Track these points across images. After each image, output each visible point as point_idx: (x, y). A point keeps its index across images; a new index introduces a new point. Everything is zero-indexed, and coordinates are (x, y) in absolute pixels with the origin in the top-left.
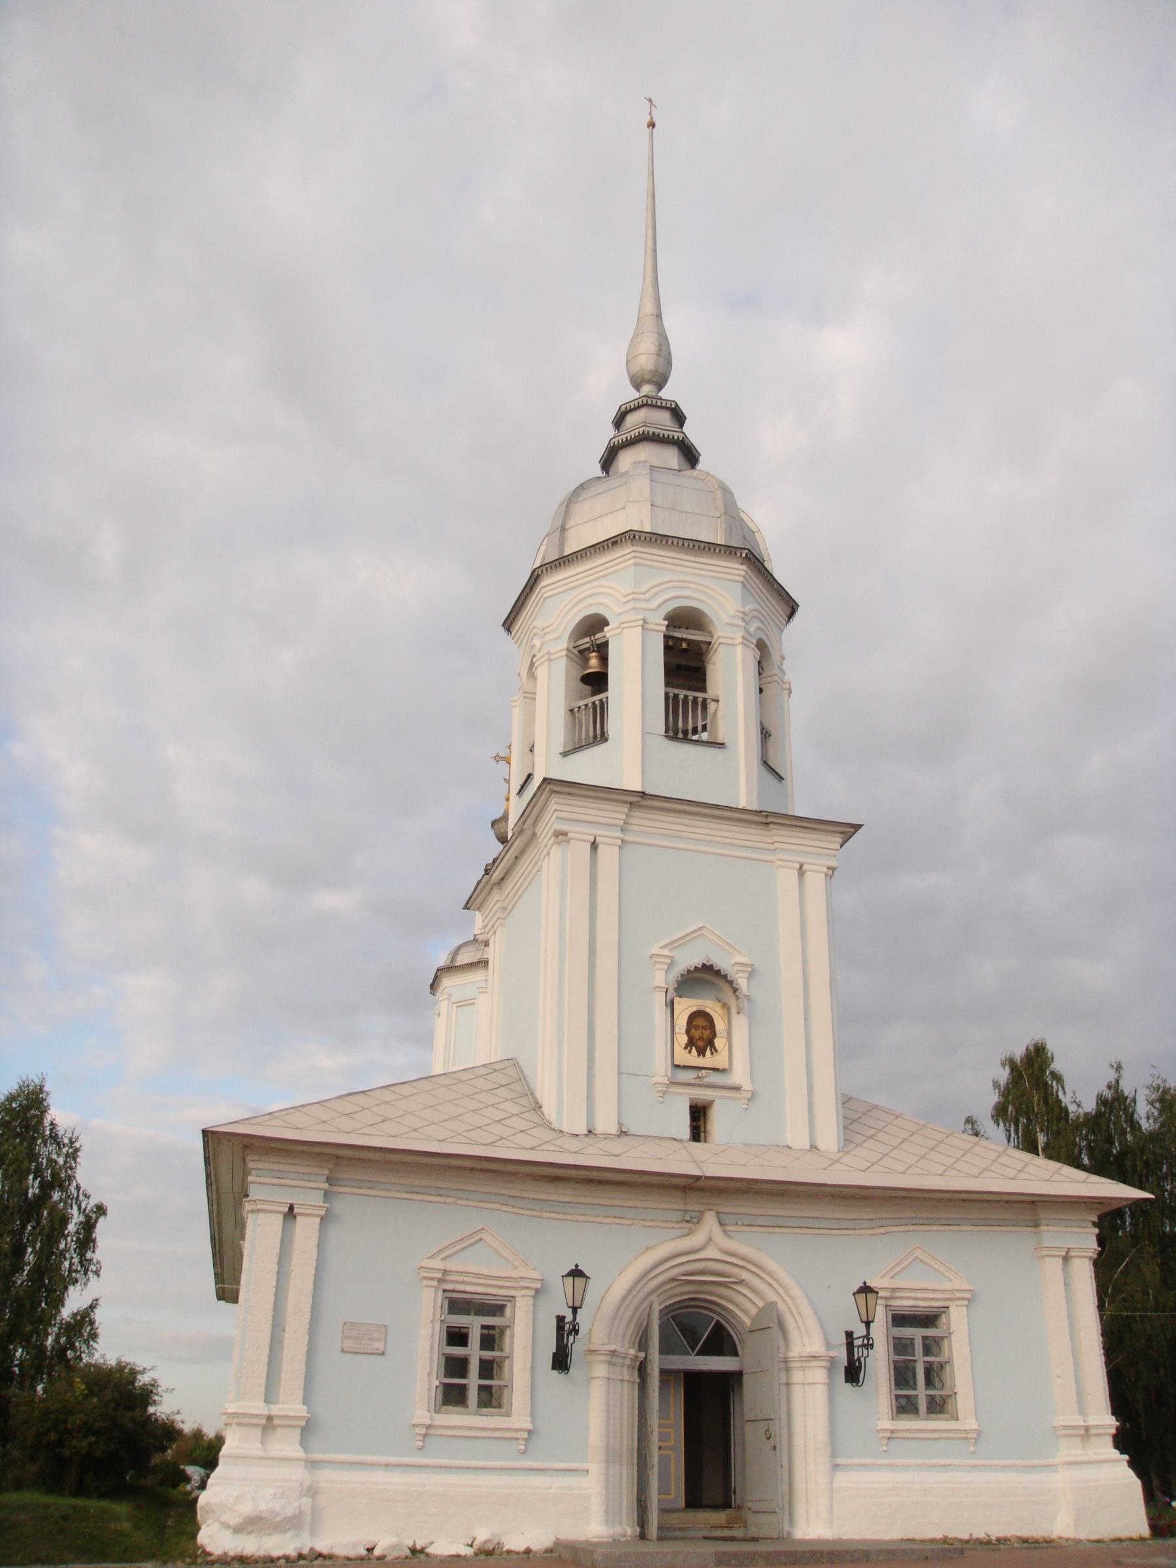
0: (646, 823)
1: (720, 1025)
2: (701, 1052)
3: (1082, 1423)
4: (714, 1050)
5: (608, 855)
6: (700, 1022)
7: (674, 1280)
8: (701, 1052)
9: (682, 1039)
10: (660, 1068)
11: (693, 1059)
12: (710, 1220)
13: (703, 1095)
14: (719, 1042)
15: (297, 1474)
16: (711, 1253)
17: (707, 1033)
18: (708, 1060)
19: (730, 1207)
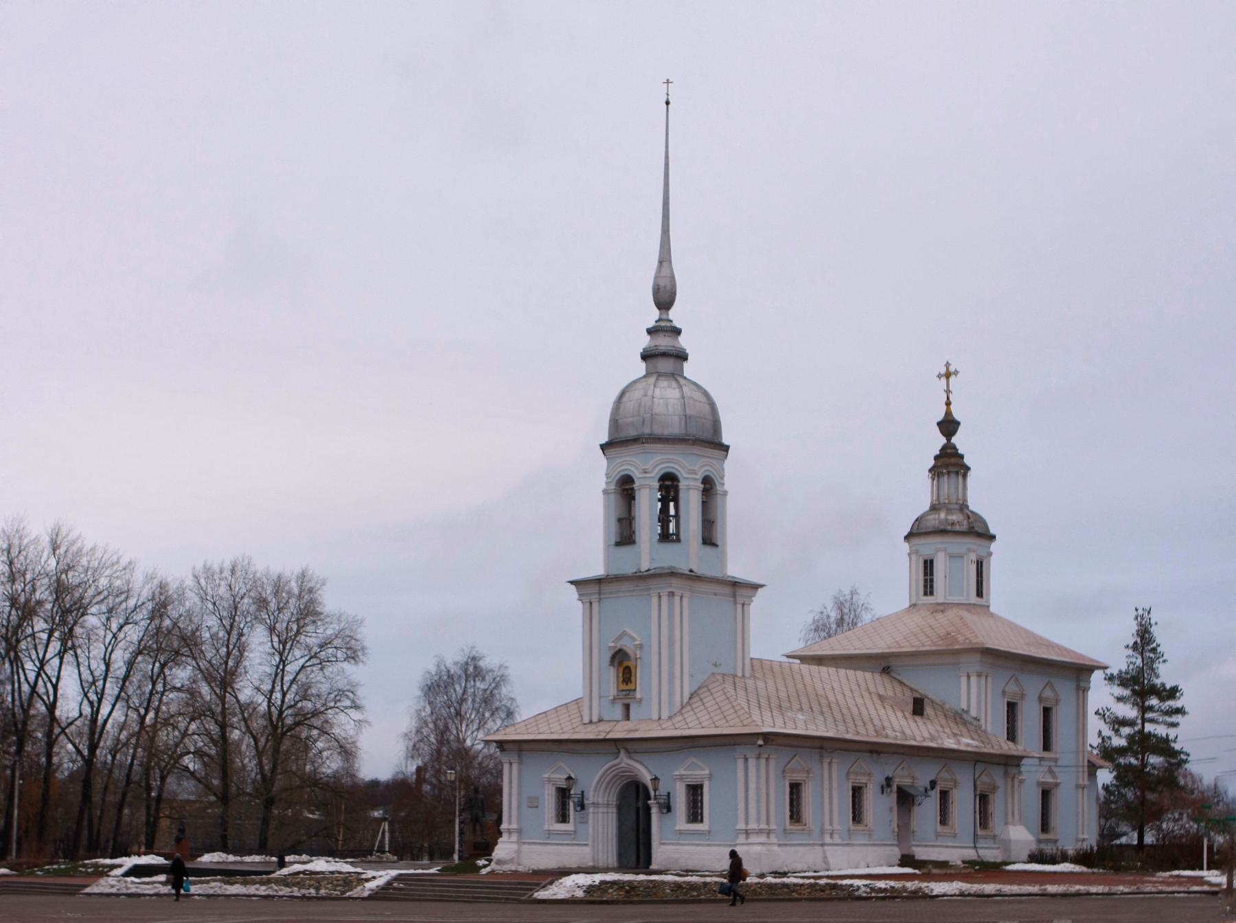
0: (606, 588)
1: (633, 671)
2: (627, 684)
3: (744, 828)
4: (631, 682)
5: (595, 605)
6: (627, 671)
7: (616, 775)
8: (627, 684)
9: (621, 679)
10: (613, 691)
11: (624, 687)
12: (623, 754)
13: (627, 701)
14: (633, 679)
15: (515, 846)
16: (623, 765)
17: (628, 676)
18: (630, 687)
19: (630, 746)
